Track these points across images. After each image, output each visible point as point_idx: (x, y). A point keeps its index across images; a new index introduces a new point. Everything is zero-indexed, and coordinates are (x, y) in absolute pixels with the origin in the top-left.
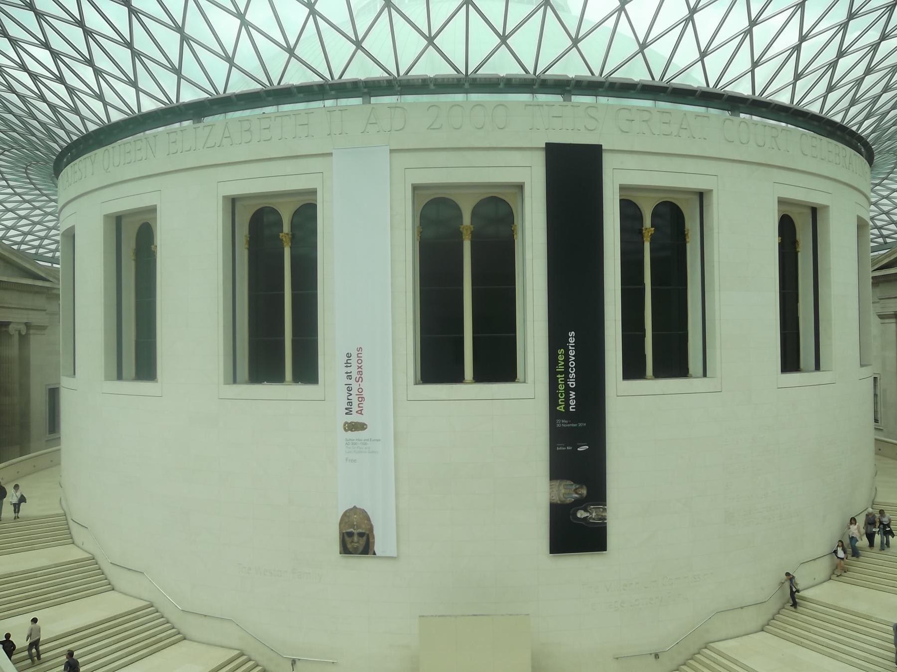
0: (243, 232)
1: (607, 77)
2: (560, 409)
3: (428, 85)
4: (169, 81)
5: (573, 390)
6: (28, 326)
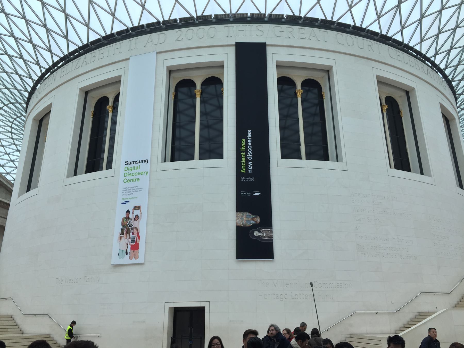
5: (250, 161)
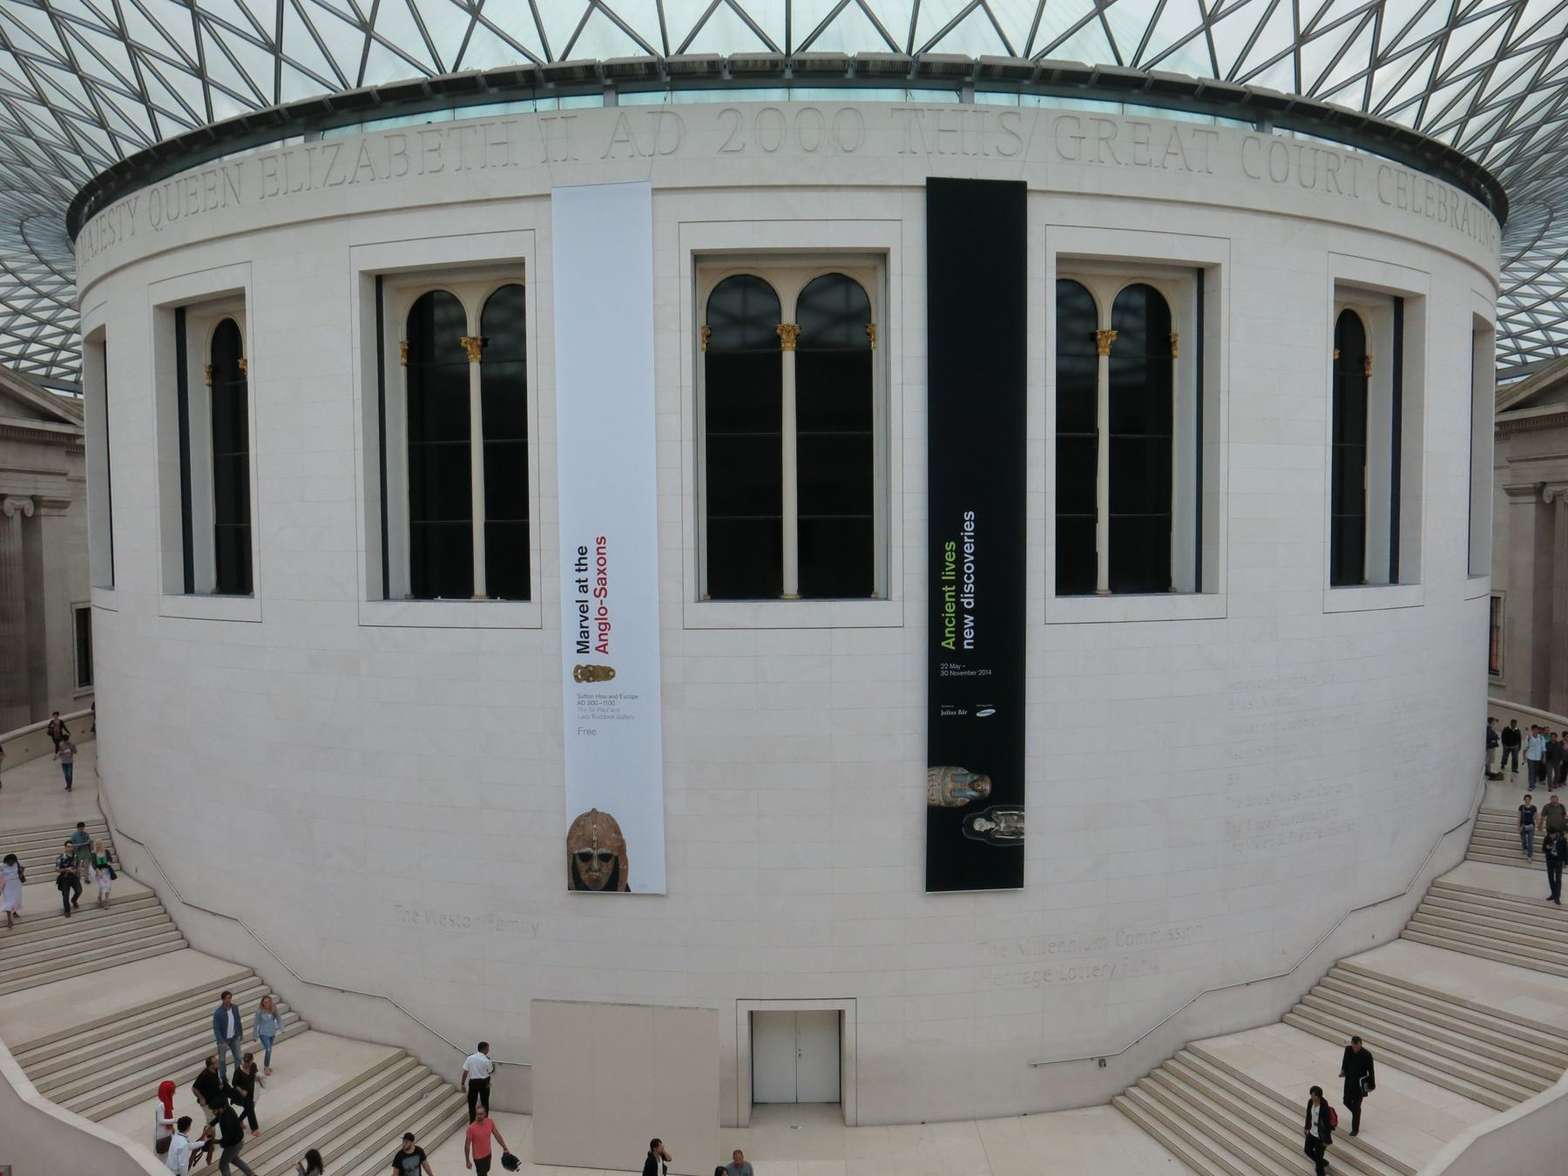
0: (396, 336)
1: (1037, 60)
2: (947, 646)
3: (720, 73)
4: (260, 64)
5: (969, 612)
6: (36, 501)
